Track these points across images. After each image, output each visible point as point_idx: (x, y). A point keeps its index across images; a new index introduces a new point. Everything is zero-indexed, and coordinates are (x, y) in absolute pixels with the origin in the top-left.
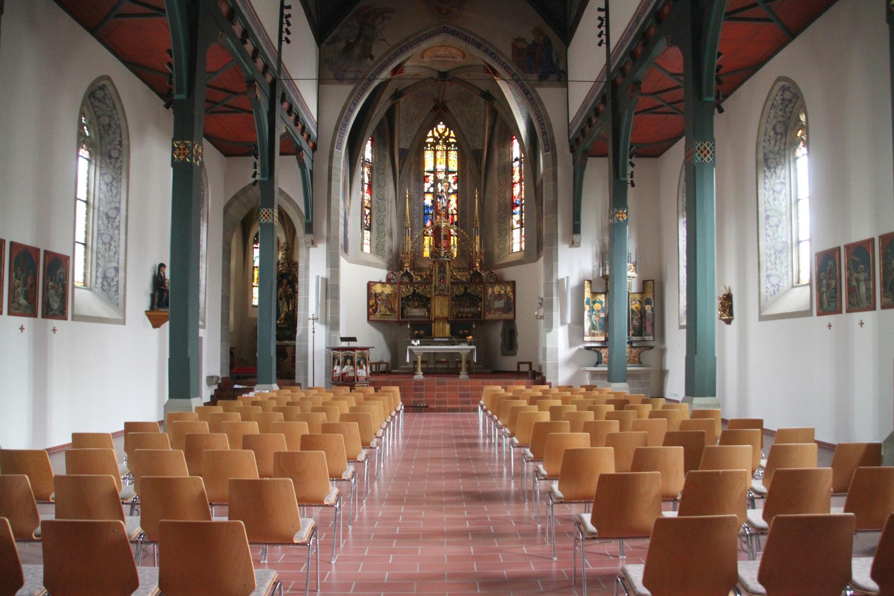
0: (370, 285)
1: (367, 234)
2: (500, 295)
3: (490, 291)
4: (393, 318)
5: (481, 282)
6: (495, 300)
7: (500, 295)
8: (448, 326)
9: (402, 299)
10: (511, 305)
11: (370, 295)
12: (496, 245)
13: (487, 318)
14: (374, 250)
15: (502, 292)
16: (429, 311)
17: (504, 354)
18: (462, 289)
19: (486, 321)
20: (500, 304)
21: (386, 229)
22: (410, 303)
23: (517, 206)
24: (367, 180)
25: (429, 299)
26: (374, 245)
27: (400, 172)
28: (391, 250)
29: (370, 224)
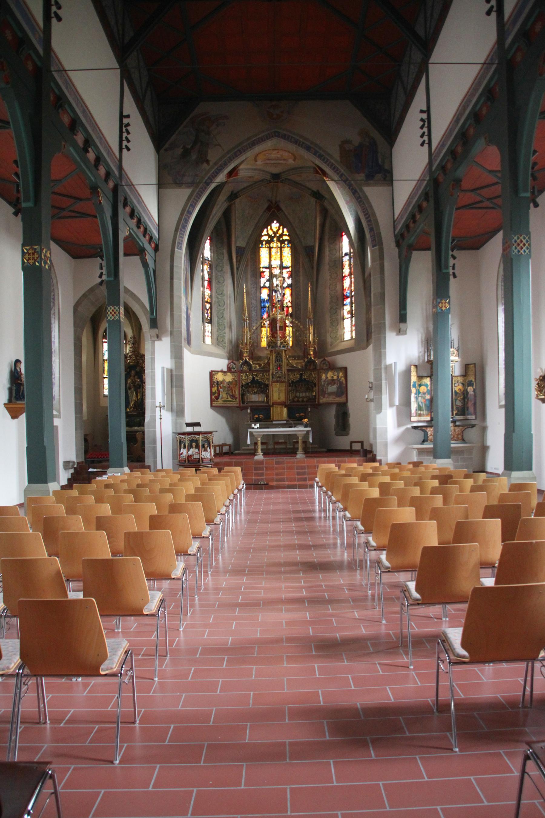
21: (226, 322)
22: (250, 389)
26: (215, 337)
29: (211, 318)
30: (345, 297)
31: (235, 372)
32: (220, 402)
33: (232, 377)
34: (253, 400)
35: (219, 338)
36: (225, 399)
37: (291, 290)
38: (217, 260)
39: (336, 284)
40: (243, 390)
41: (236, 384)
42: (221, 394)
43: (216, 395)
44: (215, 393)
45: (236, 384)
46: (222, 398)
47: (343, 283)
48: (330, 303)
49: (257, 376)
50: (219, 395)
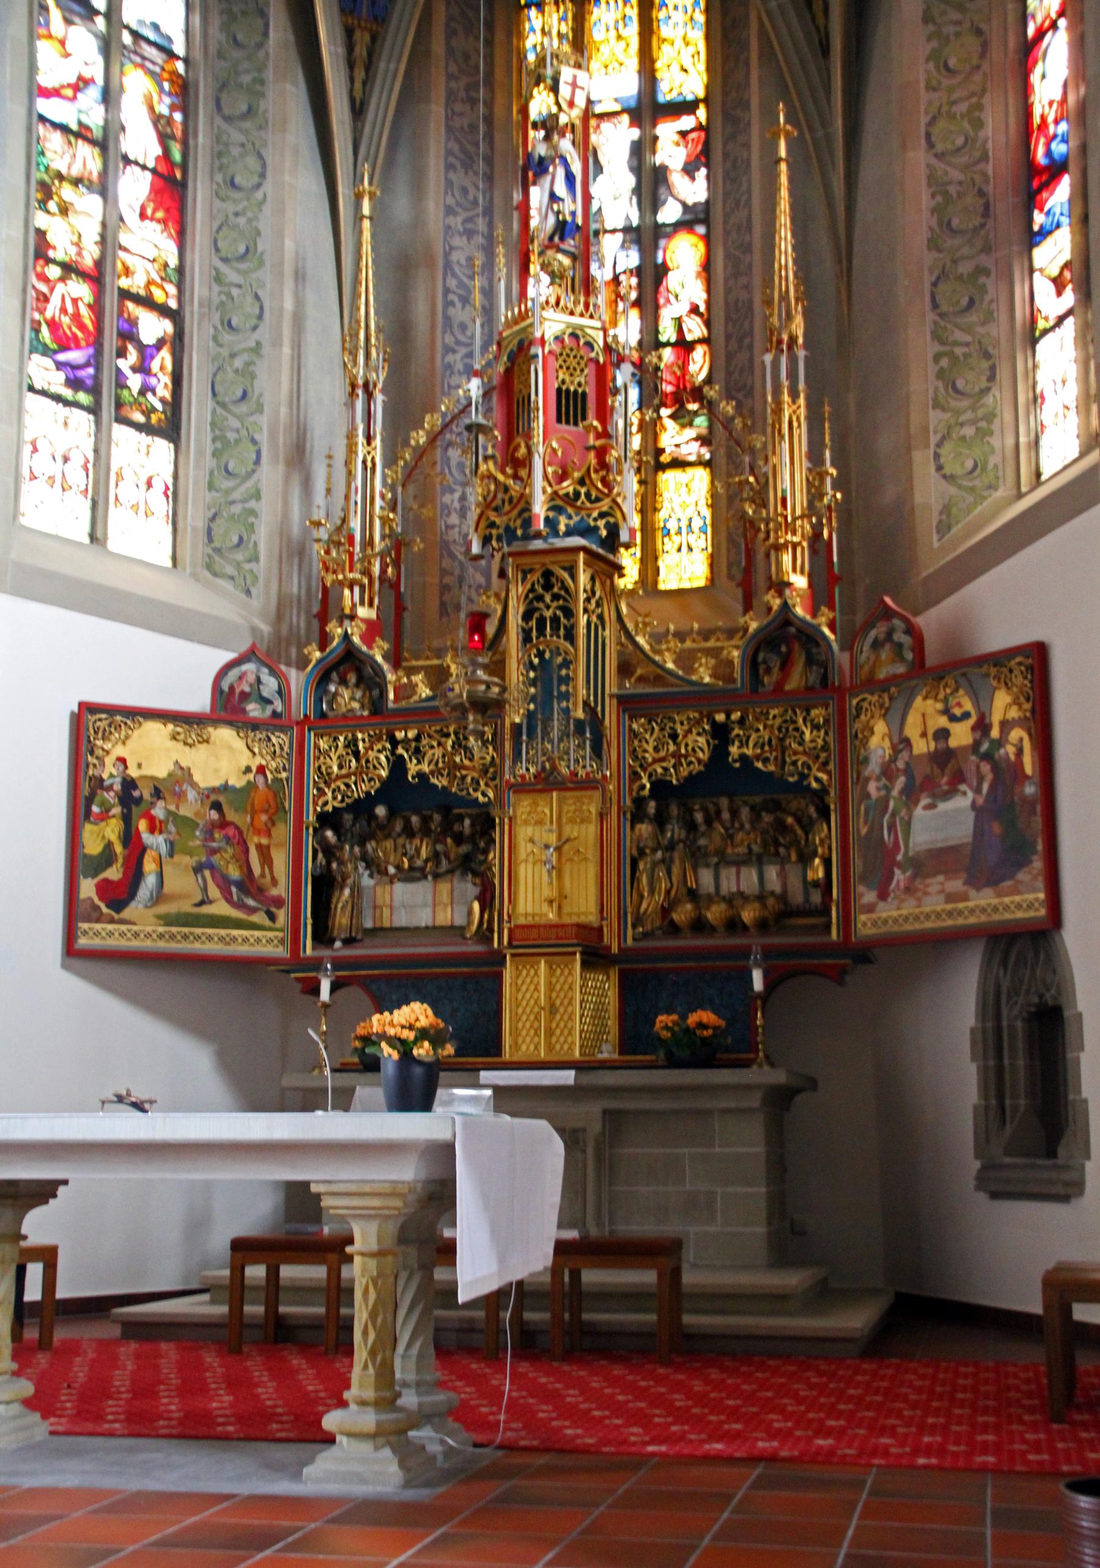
0: (91, 724)
1: (141, 457)
2: (944, 757)
4: (264, 942)
5: (825, 687)
6: (911, 795)
7: (944, 757)
9: (326, 820)
10: (1023, 826)
11: (83, 798)
12: (922, 461)
13: (865, 926)
14: (193, 548)
15: (961, 735)
16: (486, 898)
17: (998, 1185)
18: (700, 743)
20: (946, 820)
21: (269, 424)
22: (382, 849)
23: (1056, 169)
24: (141, 142)
25: (486, 823)
26: (194, 518)
27: (358, 110)
29: (175, 405)
30: (1037, 179)
31: (277, 723)
32: (140, 927)
33: (245, 759)
34: (402, 919)
35: (219, 527)
36: (186, 907)
37: (707, 239)
38: (220, 55)
39: (980, 107)
40: (329, 851)
41: (275, 810)
42: (149, 866)
43: (114, 873)
44: (108, 857)
45: (275, 810)
46: (159, 896)
47: (1026, 89)
48: (933, 244)
49: (418, 753)
50: (134, 874)
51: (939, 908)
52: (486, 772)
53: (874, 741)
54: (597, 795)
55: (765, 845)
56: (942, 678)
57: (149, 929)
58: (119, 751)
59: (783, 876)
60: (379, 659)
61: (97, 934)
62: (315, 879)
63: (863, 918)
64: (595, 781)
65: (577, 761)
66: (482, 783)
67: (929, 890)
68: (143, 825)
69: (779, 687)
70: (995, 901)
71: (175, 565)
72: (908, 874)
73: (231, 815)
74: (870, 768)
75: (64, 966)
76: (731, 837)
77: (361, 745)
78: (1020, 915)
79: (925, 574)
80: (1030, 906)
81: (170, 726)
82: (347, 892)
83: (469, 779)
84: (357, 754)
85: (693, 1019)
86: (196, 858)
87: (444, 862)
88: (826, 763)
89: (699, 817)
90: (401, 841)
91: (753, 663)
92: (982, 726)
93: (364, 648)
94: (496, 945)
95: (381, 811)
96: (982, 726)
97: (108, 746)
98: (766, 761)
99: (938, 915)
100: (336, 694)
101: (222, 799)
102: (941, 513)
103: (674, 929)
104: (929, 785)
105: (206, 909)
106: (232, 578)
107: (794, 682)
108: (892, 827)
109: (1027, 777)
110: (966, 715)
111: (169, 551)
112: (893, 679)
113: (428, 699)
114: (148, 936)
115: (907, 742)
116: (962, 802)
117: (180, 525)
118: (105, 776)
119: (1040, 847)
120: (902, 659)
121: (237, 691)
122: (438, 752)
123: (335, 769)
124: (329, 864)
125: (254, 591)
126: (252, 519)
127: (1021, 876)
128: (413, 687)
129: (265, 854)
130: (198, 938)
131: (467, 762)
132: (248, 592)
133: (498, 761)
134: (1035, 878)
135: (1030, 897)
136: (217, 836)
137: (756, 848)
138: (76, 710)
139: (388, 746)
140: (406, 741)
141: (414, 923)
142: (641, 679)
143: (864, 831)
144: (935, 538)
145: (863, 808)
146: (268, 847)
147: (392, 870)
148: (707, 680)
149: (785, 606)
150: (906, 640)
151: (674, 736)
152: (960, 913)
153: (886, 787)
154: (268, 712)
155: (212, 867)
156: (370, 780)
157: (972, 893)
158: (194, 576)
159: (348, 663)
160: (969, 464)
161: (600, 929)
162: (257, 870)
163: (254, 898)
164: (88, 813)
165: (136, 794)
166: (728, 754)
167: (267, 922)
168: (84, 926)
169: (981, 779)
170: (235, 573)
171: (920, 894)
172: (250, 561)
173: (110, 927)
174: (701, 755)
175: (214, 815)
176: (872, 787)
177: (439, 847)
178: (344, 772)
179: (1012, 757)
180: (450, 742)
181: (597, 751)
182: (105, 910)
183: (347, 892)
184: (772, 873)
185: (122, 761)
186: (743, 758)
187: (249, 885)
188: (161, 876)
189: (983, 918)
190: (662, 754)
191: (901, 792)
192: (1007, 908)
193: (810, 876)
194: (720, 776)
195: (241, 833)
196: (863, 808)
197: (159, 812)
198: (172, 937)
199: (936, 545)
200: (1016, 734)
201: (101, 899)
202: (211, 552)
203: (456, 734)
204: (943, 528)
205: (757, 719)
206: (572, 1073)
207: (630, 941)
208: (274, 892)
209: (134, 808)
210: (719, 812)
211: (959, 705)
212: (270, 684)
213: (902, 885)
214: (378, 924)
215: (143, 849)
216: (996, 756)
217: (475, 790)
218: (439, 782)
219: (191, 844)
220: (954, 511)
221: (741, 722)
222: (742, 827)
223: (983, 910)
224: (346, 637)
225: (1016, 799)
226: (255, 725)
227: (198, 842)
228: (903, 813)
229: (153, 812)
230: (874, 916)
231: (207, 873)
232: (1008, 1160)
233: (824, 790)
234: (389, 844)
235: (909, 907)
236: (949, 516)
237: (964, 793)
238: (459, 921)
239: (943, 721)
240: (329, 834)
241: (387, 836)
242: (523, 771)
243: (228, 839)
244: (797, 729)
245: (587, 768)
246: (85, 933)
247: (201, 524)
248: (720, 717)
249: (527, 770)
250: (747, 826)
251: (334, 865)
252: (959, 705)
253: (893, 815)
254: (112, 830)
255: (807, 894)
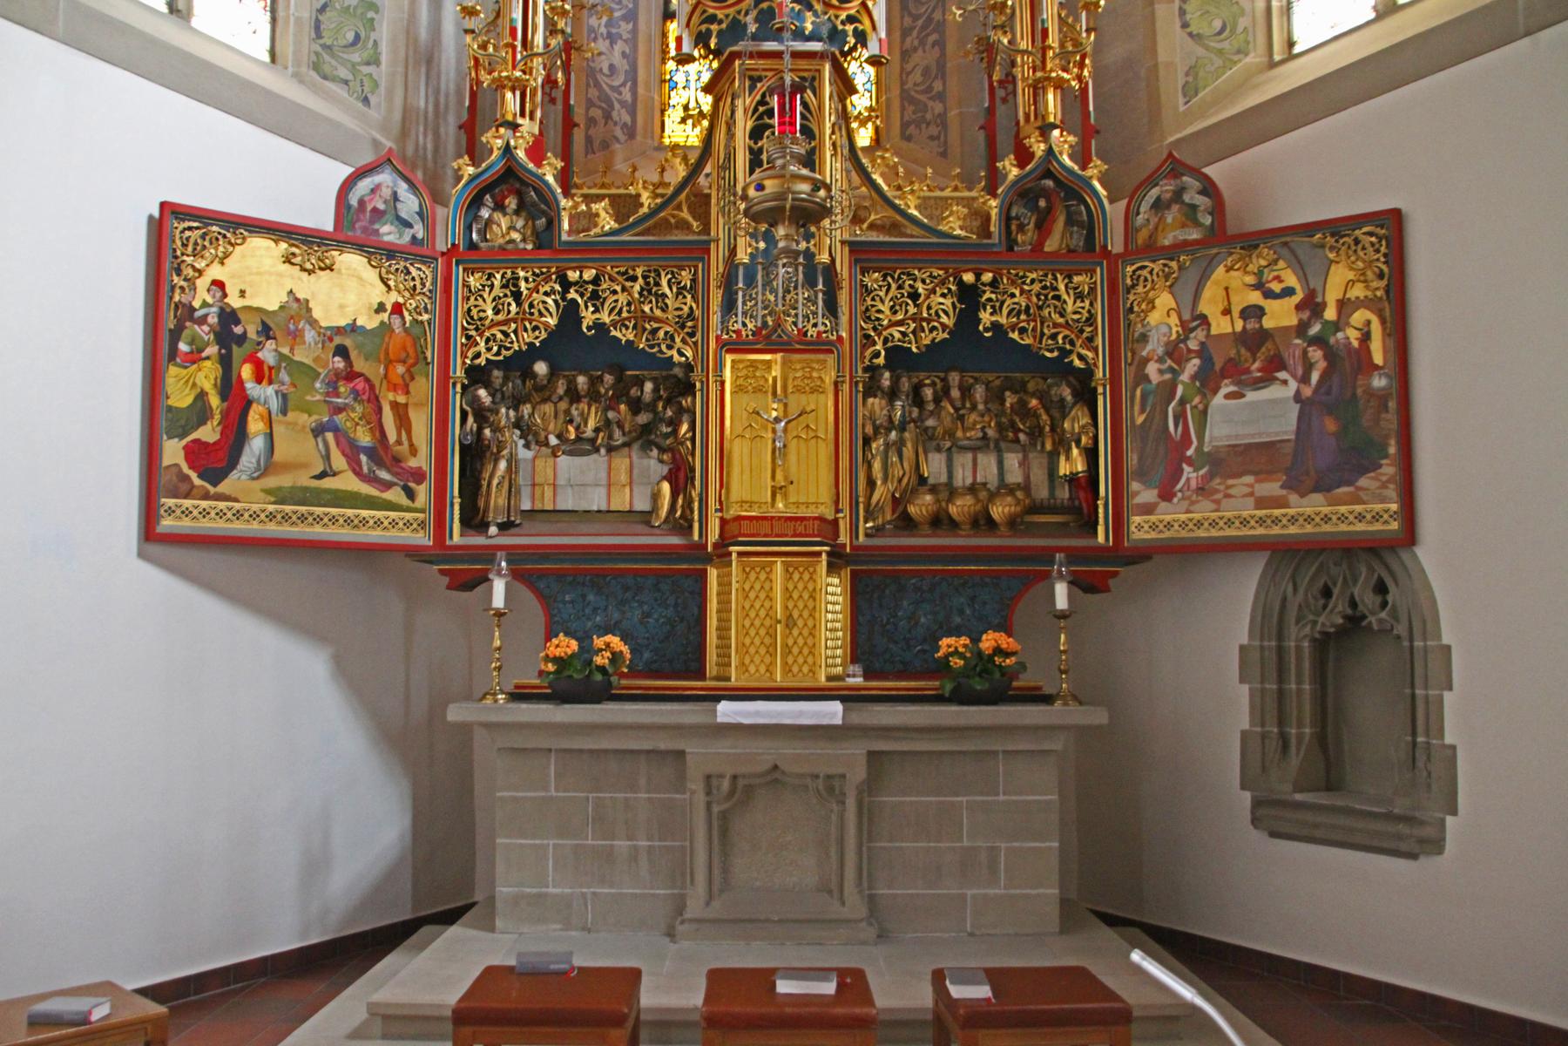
0: (178, 235)
2: (1254, 339)
3: (1161, 316)
4: (400, 523)
5: (1090, 249)
6: (1207, 381)
7: (1254, 339)
8: (834, 592)
9: (477, 375)
10: (1362, 420)
11: (166, 330)
13: (1140, 529)
14: (295, 42)
15: (1281, 315)
16: (680, 476)
17: (1272, 815)
18: (944, 305)
19: (1142, 554)
20: (1268, 410)
22: (542, 415)
25: (680, 386)
28: (425, 58)
31: (417, 252)
32: (244, 502)
33: (377, 293)
34: (567, 502)
36: (304, 480)
40: (482, 415)
42: (255, 425)
43: (208, 433)
44: (200, 411)
46: (268, 465)
50: (235, 433)
51: (1245, 514)
52: (683, 327)
53: (1154, 318)
54: (831, 360)
55: (1000, 428)
56: (1256, 247)
57: (255, 507)
58: (216, 272)
59: (1024, 463)
60: (550, 179)
61: (187, 513)
62: (464, 449)
63: (1137, 519)
64: (831, 343)
65: (806, 317)
66: (678, 340)
67: (1232, 491)
68: (247, 372)
69: (1038, 247)
70: (1326, 510)
71: (273, 60)
72: (1202, 472)
73: (360, 365)
74: (1149, 347)
75: (141, 555)
76: (961, 418)
77: (523, 285)
78: (1360, 527)
79: (1171, 139)
80: (1376, 517)
81: (283, 245)
82: (503, 465)
83: (661, 334)
84: (517, 295)
85: (988, 641)
86: (315, 417)
87: (617, 433)
88: (1090, 339)
89: (928, 393)
90: (563, 405)
91: (1007, 218)
92: (1312, 305)
93: (531, 166)
94: (696, 537)
95: (541, 368)
96: (1312, 305)
97: (200, 264)
98: (1023, 331)
99: (1244, 522)
100: (489, 222)
101: (348, 342)
102: (1187, 74)
103: (906, 523)
104: (1233, 370)
105: (327, 483)
106: (346, 82)
107: (1051, 245)
108: (1180, 416)
109: (1377, 367)
110: (1289, 292)
111: (268, 46)
112: (1182, 246)
113: (612, 233)
114: (254, 516)
115: (1204, 320)
116: (1284, 390)
117: (281, 13)
118: (196, 304)
119: (1392, 450)
120: (1197, 224)
121: (369, 208)
122: (623, 298)
123: (490, 312)
124: (480, 430)
125: (373, 100)
126: (370, 14)
127: (1363, 482)
128: (593, 217)
129: (401, 413)
130: (318, 519)
131: (658, 313)
132: (366, 101)
133: (697, 313)
134: (1384, 486)
135: (1378, 507)
136: (342, 389)
137: (991, 433)
138: (156, 214)
139: (558, 287)
140: (581, 283)
141: (583, 506)
142: (872, 227)
143: (1140, 420)
144: (1181, 100)
145: (1138, 392)
146: (406, 405)
147: (553, 441)
148: (958, 232)
149: (1050, 151)
150: (1202, 201)
151: (914, 296)
152: (1276, 521)
153: (1171, 370)
154: (406, 239)
155: (336, 430)
156: (535, 328)
157: (1293, 498)
158: (297, 76)
159: (508, 183)
160: (1217, 24)
161: (836, 521)
162: (392, 436)
163: (389, 471)
164: (173, 353)
165: (238, 330)
166: (979, 321)
167: (405, 501)
168: (171, 502)
169: (1309, 367)
170: (350, 77)
171: (1218, 496)
172: (368, 64)
173: (204, 504)
174: (944, 319)
175: (339, 363)
176: (1152, 369)
177: (611, 415)
178: (500, 317)
179: (1355, 344)
180: (637, 288)
181: (832, 308)
182: (197, 481)
183: (503, 465)
184: (1012, 460)
185: (219, 284)
186: (996, 326)
187: (382, 453)
188: (270, 437)
189: (1309, 529)
190: (900, 317)
191: (1194, 377)
192: (1342, 518)
193: (1064, 469)
194: (968, 346)
195: (372, 387)
196: (1138, 392)
197: (267, 355)
198: (286, 518)
199: (1182, 108)
200: (1359, 317)
201: (191, 467)
202: (319, 49)
203: (645, 277)
204: (1190, 91)
205: (1013, 283)
206: (836, 707)
207: (861, 538)
208: (413, 463)
209: (235, 347)
210: (946, 391)
211: (1278, 279)
212: (409, 204)
213: (1193, 484)
214: (538, 506)
215: (248, 403)
216: (1332, 340)
217: (670, 347)
218: (624, 335)
219: (308, 398)
220: (1201, 74)
221: (994, 284)
222: (974, 407)
223: (1309, 520)
224: (507, 150)
225: (1359, 391)
226: (391, 252)
227: (318, 397)
228: (1197, 400)
229: (260, 355)
230: (1153, 518)
231: (330, 436)
232: (1299, 797)
233: (1088, 373)
234: (548, 408)
235: (1203, 511)
236: (1196, 78)
237: (1285, 382)
238: (642, 504)
239: (1255, 297)
240: (482, 393)
241: (545, 400)
242: (738, 326)
243: (356, 394)
244: (1057, 298)
245: (817, 327)
246: (170, 511)
247: (306, 15)
248: (968, 278)
249: (746, 325)
250: (981, 407)
251: (487, 432)
252: (1278, 279)
253: (1182, 402)
254: (207, 376)
255: (1052, 488)
